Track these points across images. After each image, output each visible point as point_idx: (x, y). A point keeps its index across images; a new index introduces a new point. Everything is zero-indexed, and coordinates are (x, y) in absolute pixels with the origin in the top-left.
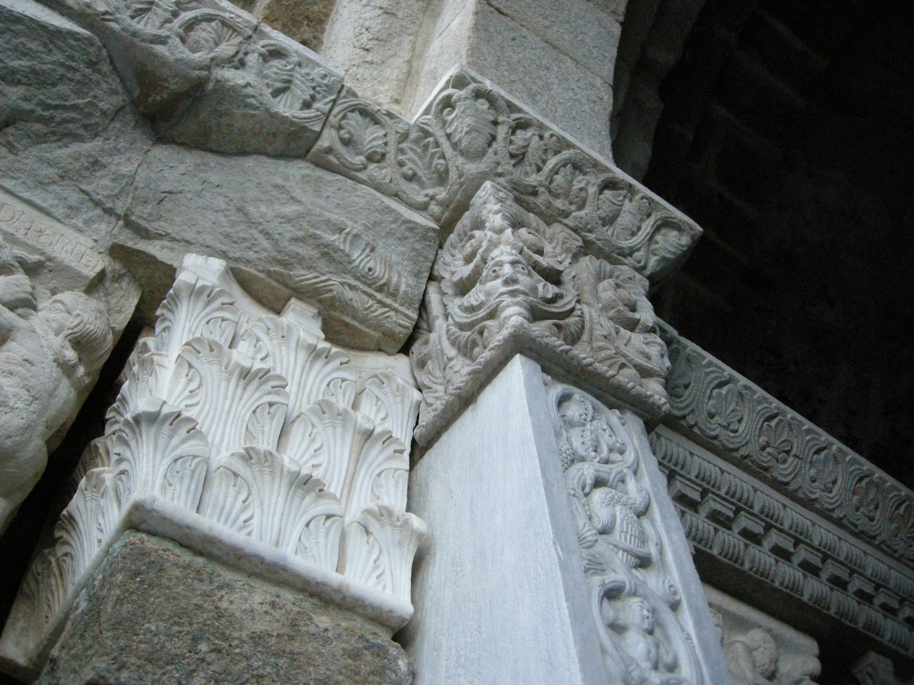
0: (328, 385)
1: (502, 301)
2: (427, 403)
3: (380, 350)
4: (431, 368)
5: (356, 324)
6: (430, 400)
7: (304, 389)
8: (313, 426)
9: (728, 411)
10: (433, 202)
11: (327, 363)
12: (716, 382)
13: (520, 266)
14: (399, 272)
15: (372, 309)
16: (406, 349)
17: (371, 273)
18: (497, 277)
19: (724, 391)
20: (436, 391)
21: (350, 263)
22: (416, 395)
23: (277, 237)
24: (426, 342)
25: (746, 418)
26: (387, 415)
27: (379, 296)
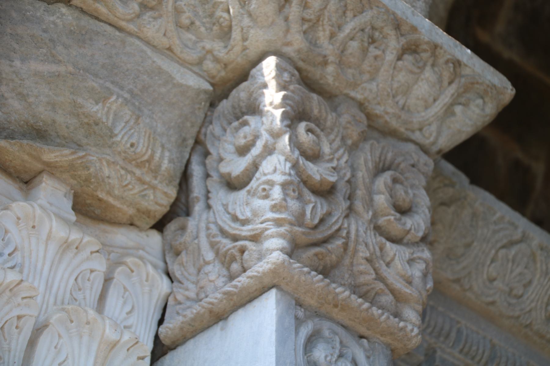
0: (76, 279)
1: (267, 229)
2: (176, 299)
3: (132, 224)
4: (185, 260)
5: (111, 200)
6: (180, 297)
7: (52, 287)
8: (60, 336)
9: (514, 274)
10: (209, 56)
11: (76, 254)
12: (505, 241)
13: (291, 188)
14: (163, 146)
15: (130, 187)
16: (160, 226)
17: (132, 149)
18: (266, 197)
19: (513, 251)
20: (187, 289)
21: (111, 137)
22: (164, 285)
23: (32, 100)
24: (183, 228)
25: (535, 282)
26: (133, 308)
27: (138, 172)
